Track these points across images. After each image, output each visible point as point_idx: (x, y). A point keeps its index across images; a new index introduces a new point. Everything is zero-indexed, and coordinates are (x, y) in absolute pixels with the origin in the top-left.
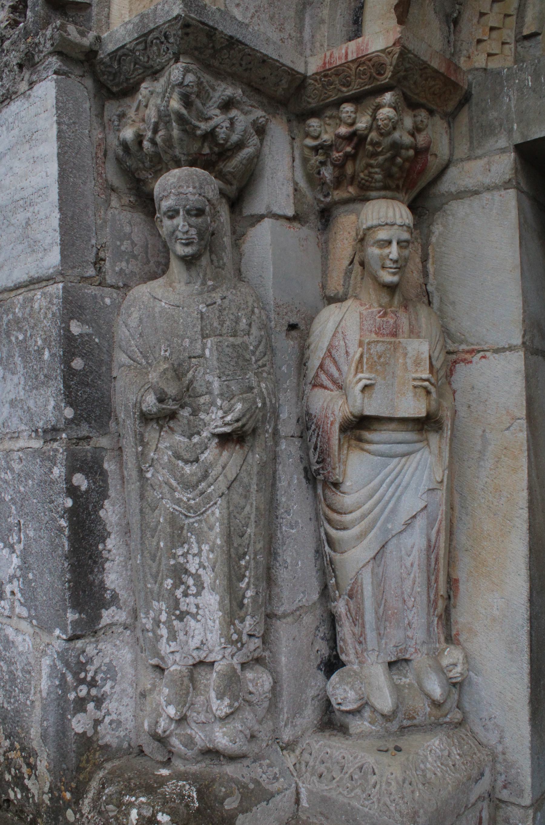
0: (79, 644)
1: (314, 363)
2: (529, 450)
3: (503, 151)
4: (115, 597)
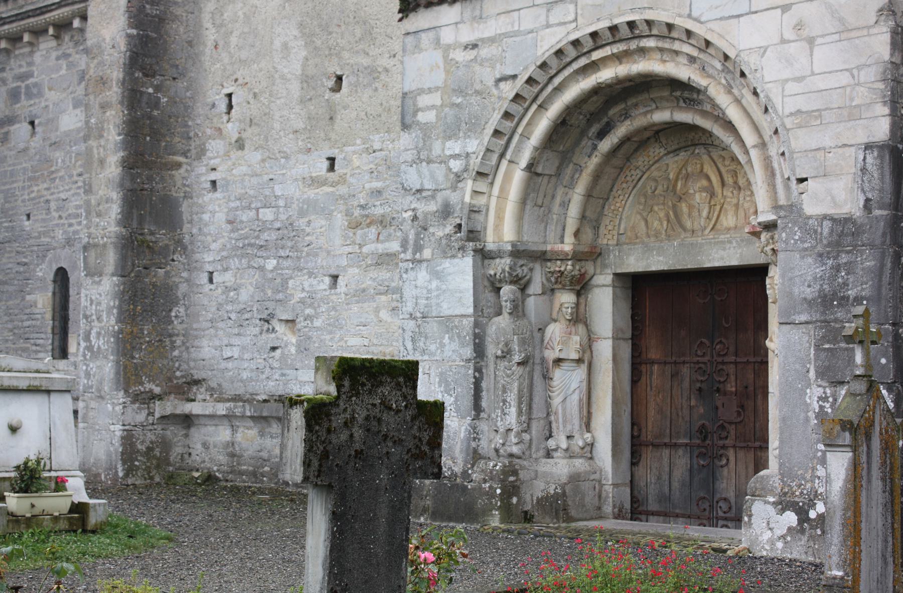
0: (475, 421)
1: (546, 342)
2: (613, 370)
3: (610, 274)
4: (484, 410)
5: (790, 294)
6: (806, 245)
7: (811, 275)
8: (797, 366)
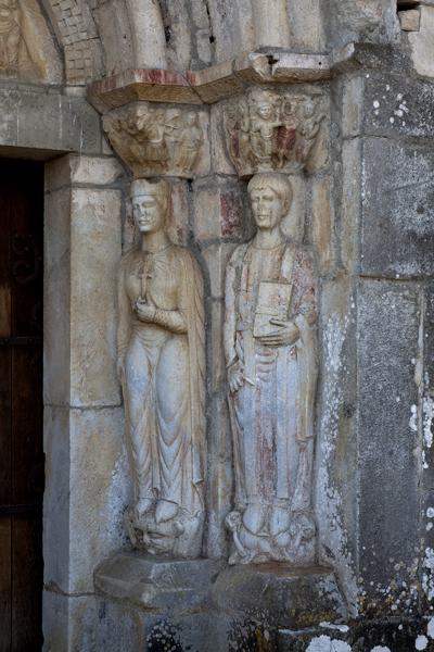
5: (386, 224)
6: (417, 132)
7: (425, 190)
8: (394, 362)
